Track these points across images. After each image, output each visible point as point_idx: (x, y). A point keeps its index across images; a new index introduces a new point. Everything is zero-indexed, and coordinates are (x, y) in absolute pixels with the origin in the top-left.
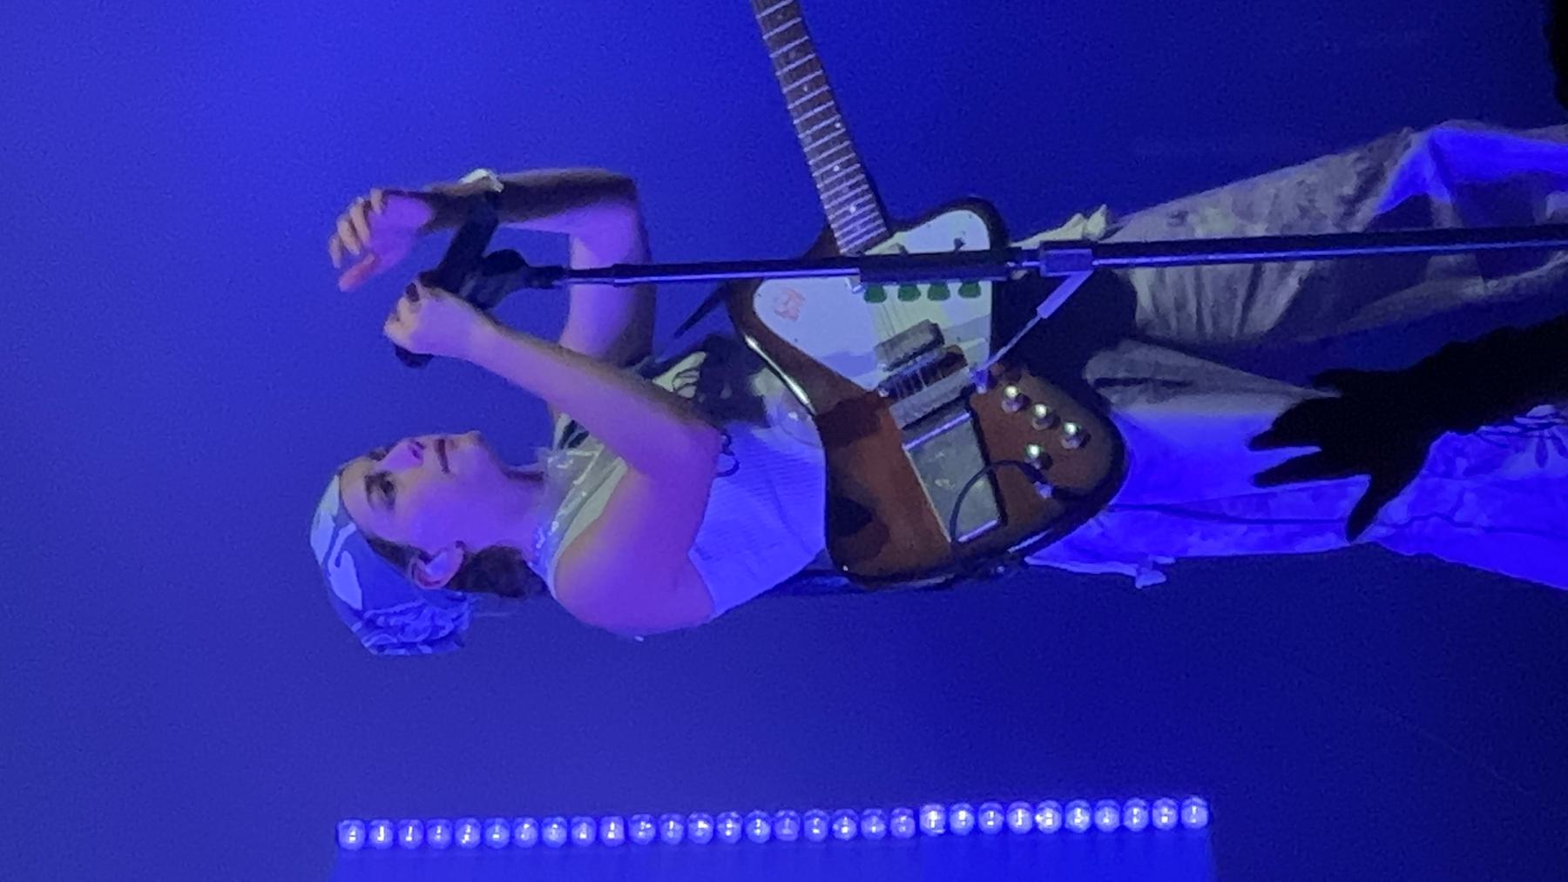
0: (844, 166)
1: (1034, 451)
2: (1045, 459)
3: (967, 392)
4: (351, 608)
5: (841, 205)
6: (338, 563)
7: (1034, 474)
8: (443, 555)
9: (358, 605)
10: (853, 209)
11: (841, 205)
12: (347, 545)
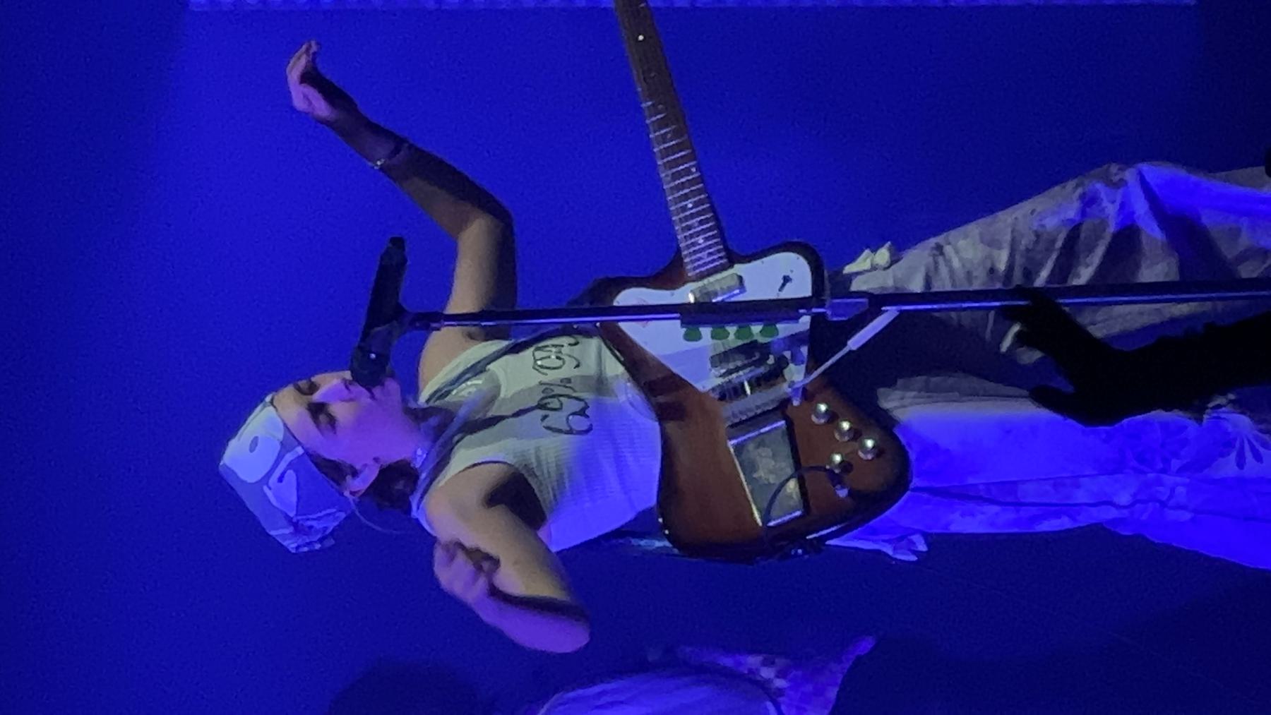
0: (696, 205)
1: (838, 458)
2: (846, 466)
3: (785, 403)
4: (287, 516)
5: (691, 236)
6: (280, 479)
7: (835, 479)
8: (367, 471)
9: (292, 514)
10: (701, 241)
11: (691, 236)
12: (290, 465)
